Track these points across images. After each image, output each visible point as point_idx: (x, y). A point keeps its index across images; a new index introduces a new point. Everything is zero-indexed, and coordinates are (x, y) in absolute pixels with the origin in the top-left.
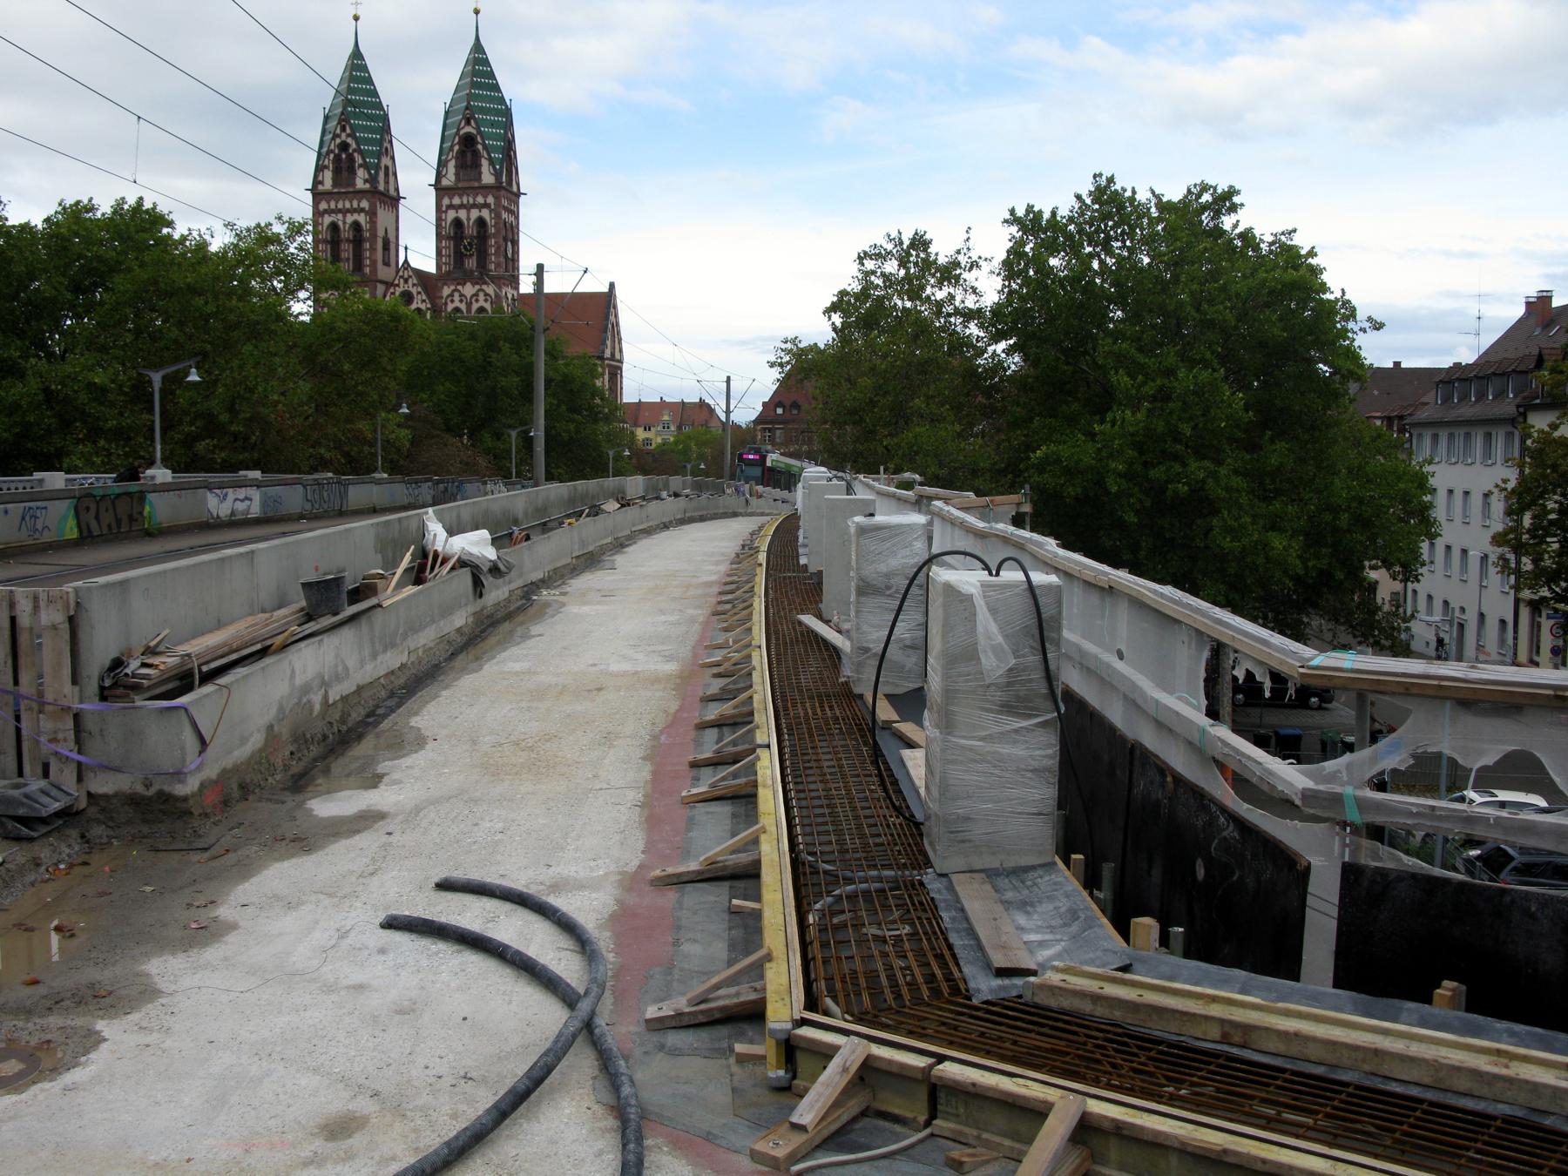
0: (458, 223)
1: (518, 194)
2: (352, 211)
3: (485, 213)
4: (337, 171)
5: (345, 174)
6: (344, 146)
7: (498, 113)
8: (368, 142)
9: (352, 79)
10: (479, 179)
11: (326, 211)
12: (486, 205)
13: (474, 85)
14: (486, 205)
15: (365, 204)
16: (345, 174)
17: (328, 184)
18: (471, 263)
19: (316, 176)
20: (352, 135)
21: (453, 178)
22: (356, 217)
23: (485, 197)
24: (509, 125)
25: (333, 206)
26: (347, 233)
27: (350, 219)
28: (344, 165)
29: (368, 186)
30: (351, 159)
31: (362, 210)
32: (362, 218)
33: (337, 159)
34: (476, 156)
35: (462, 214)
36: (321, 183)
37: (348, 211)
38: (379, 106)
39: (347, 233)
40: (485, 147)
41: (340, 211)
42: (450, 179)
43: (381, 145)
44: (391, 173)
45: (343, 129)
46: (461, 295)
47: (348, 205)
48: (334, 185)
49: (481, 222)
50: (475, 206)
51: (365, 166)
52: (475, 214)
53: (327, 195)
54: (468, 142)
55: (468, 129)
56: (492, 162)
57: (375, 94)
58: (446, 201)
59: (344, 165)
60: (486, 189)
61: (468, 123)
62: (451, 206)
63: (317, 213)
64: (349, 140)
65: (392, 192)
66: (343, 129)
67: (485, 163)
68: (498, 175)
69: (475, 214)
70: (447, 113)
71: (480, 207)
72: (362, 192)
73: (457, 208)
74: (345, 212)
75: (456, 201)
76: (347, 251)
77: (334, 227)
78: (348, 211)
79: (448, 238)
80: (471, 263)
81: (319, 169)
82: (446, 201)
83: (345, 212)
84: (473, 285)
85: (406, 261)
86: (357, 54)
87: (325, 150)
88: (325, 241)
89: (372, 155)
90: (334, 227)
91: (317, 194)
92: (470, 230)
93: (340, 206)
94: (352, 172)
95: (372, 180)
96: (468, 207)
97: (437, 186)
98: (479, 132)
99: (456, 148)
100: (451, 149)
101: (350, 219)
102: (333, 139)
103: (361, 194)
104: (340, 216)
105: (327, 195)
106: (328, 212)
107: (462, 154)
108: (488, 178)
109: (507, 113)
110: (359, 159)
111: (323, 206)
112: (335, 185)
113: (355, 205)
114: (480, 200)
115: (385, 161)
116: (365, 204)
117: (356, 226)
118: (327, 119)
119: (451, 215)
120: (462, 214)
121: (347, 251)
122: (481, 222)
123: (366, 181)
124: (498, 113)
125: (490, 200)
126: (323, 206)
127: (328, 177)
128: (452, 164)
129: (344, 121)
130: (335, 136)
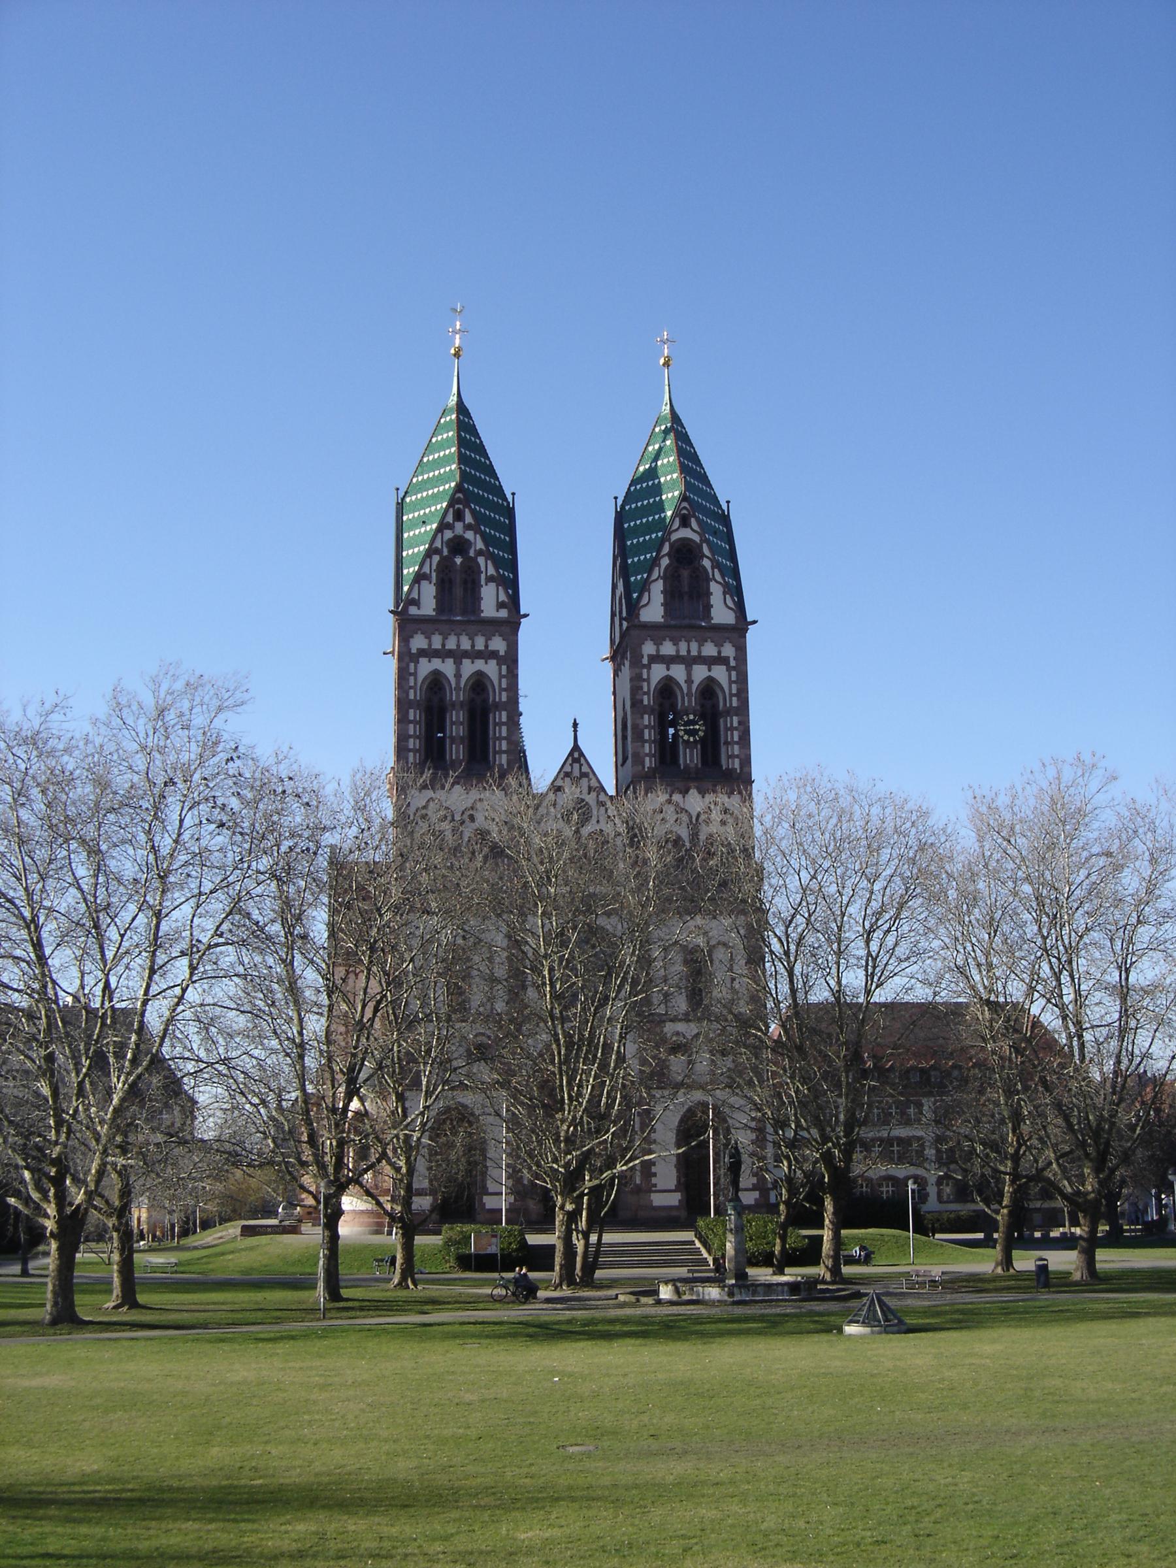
0: (667, 688)
2: (475, 655)
5: (458, 591)
6: (459, 546)
11: (422, 653)
12: (720, 660)
15: (498, 644)
16: (458, 591)
17: (428, 606)
18: (689, 758)
21: (661, 611)
22: (480, 665)
23: (719, 645)
27: (469, 668)
28: (458, 579)
29: (503, 613)
31: (494, 655)
32: (491, 669)
33: (445, 568)
35: (678, 672)
36: (416, 603)
37: (466, 654)
40: (716, 565)
41: (449, 654)
42: (653, 611)
45: (459, 516)
46: (680, 810)
47: (466, 644)
52: (700, 673)
59: (458, 579)
62: (656, 658)
63: (406, 659)
64: (469, 535)
66: (459, 516)
67: (716, 590)
69: (700, 673)
71: (710, 662)
73: (668, 661)
74: (458, 656)
75: (668, 649)
76: (456, 725)
77: (436, 682)
78: (466, 654)
80: (689, 758)
82: (648, 648)
83: (458, 656)
84: (702, 792)
90: (436, 682)
91: (407, 621)
92: (687, 700)
93: (451, 644)
96: (689, 662)
98: (708, 541)
99: (665, 562)
100: (655, 562)
101: (469, 668)
102: (440, 530)
103: (493, 626)
104: (450, 661)
108: (721, 614)
110: (487, 568)
111: (418, 642)
114: (710, 650)
116: (498, 644)
117: (479, 683)
119: (658, 672)
120: (678, 672)
121: (456, 725)
122: (709, 689)
123: (500, 605)
125: (728, 651)
126: (418, 642)
127: (429, 592)
128: (657, 588)
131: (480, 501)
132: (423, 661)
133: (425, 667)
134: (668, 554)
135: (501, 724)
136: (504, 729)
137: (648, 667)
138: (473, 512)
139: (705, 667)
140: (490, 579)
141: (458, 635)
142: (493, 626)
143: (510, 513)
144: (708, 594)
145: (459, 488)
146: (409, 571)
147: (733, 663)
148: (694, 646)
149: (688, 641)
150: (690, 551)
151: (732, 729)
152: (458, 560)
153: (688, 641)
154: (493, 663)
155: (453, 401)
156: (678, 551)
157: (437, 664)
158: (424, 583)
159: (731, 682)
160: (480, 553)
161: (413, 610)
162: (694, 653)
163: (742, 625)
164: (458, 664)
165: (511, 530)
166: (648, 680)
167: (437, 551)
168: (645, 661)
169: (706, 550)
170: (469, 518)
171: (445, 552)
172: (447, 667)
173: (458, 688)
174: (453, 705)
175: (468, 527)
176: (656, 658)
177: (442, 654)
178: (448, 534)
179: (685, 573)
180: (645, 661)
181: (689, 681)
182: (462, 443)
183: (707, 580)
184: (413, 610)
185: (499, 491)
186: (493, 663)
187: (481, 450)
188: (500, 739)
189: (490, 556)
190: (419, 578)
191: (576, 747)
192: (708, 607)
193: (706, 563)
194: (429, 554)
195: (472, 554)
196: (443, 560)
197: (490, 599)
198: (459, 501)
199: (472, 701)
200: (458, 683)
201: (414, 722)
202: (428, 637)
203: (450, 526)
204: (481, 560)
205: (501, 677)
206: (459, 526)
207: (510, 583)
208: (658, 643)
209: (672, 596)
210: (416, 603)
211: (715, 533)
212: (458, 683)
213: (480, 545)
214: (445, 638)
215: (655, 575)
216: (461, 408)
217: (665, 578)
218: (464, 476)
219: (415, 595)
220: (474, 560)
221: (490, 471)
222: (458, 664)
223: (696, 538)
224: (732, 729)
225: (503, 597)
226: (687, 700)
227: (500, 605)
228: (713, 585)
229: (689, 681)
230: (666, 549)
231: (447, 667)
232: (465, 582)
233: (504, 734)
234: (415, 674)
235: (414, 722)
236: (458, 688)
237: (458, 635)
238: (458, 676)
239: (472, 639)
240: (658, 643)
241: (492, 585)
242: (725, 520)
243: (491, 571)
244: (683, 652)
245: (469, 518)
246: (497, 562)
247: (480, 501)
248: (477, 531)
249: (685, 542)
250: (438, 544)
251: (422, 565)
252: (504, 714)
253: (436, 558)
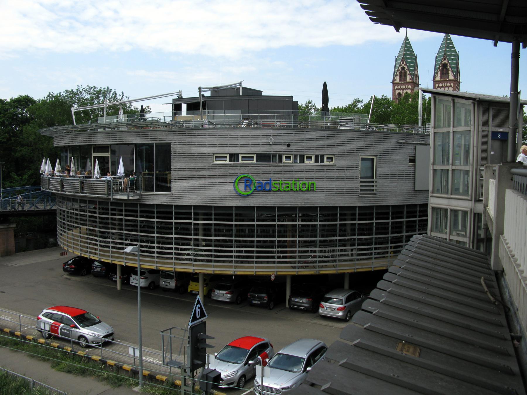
1: (460, 82)
2: (406, 89)
4: (401, 76)
5: (403, 77)
6: (403, 68)
7: (454, 56)
8: (411, 67)
9: (405, 47)
10: (448, 78)
11: (397, 89)
12: (450, 86)
13: (447, 47)
15: (410, 87)
16: (403, 77)
17: (398, 80)
19: (394, 78)
20: (406, 65)
22: (407, 90)
24: (457, 60)
25: (399, 87)
27: (405, 91)
28: (403, 75)
30: (405, 72)
31: (409, 88)
32: (409, 91)
33: (401, 72)
34: (447, 70)
36: (396, 80)
38: (414, 55)
40: (451, 67)
41: (401, 89)
42: (438, 78)
43: (414, 67)
44: (417, 76)
45: (403, 63)
47: (404, 87)
48: (400, 81)
50: (447, 86)
51: (410, 74)
53: (398, 84)
54: (445, 65)
55: (445, 62)
56: (453, 72)
57: (412, 51)
58: (437, 85)
59: (403, 75)
60: (450, 81)
61: (445, 59)
63: (394, 90)
65: (417, 83)
66: (403, 63)
67: (450, 72)
68: (454, 76)
70: (436, 56)
72: (409, 83)
75: (441, 85)
77: (399, 94)
78: (404, 89)
81: (395, 76)
82: (437, 85)
83: (403, 89)
86: (407, 39)
87: (396, 70)
88: (397, 99)
89: (412, 70)
90: (399, 94)
91: (394, 84)
93: (402, 87)
94: (405, 76)
95: (412, 79)
97: (434, 80)
98: (449, 62)
100: (439, 67)
101: (405, 91)
102: (400, 66)
105: (398, 84)
106: (398, 89)
107: (442, 70)
108: (451, 77)
109: (457, 56)
110: (408, 72)
111: (396, 87)
113: (407, 87)
114: (448, 85)
115: (416, 73)
116: (410, 87)
118: (396, 60)
124: (454, 56)
125: (452, 84)
126: (396, 87)
127: (398, 78)
128: (439, 73)
129: (403, 60)
131: (408, 59)
133: (397, 92)
155: (404, 37)
157: (399, 91)
172: (401, 91)
176: (438, 87)
177: (401, 89)
193: (449, 67)
194: (398, 71)
208: (439, 84)
209: (441, 74)
211: (453, 60)
227: (410, 79)
240: (439, 84)
247: (408, 59)
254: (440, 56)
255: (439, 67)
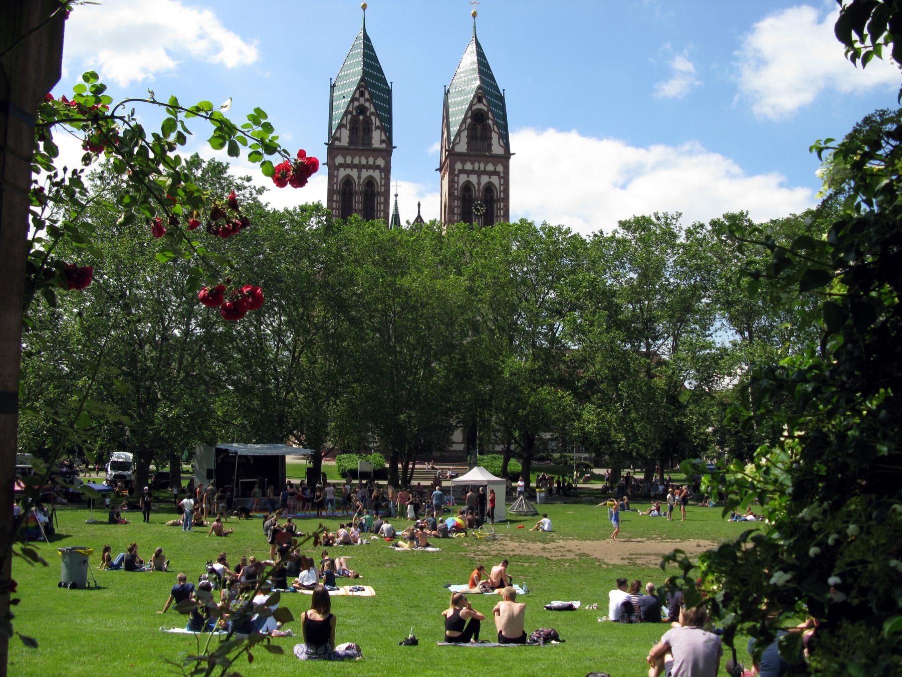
0: (467, 187)
2: (368, 167)
3: (495, 180)
4: (353, 131)
5: (361, 133)
6: (362, 110)
11: (341, 165)
12: (495, 173)
14: (495, 173)
15: (381, 162)
16: (361, 133)
17: (345, 141)
22: (370, 172)
23: (495, 165)
25: (349, 160)
26: (358, 188)
27: (365, 174)
28: (360, 127)
29: (384, 146)
31: (378, 167)
32: (376, 174)
33: (354, 121)
35: (473, 179)
36: (339, 139)
39: (358, 188)
40: (495, 123)
41: (355, 166)
45: (362, 94)
47: (364, 161)
49: (489, 188)
52: (485, 179)
53: (343, 150)
58: (458, 166)
59: (360, 127)
61: (480, 100)
62: (462, 171)
64: (367, 104)
66: (362, 94)
67: (495, 136)
69: (485, 179)
71: (490, 174)
73: (468, 173)
74: (360, 167)
75: (468, 166)
77: (348, 181)
78: (364, 167)
79: (458, 198)
82: (458, 166)
83: (360, 167)
85: (419, 219)
87: (339, 112)
88: (338, 192)
90: (348, 181)
92: (478, 194)
93: (356, 161)
94: (368, 131)
96: (479, 173)
98: (491, 111)
99: (469, 121)
101: (365, 174)
102: (352, 101)
103: (378, 152)
104: (355, 170)
105: (343, 150)
108: (497, 149)
111: (339, 160)
112: (351, 142)
114: (490, 167)
116: (381, 162)
117: (370, 182)
119: (463, 178)
120: (473, 179)
122: (489, 188)
123: (382, 142)
125: (500, 168)
126: (339, 160)
127: (345, 134)
128: (465, 134)
130: (353, 100)
132: (341, 170)
133: (342, 173)
134: (471, 117)
135: (381, 203)
136: (382, 206)
137: (458, 175)
138: (370, 93)
139: (487, 177)
140: (377, 128)
141: (360, 157)
142: (378, 152)
143: (389, 92)
144: (491, 138)
145: (362, 79)
146: (336, 123)
147: (502, 175)
148: (482, 165)
149: (479, 163)
150: (482, 115)
151: (500, 209)
152: (361, 118)
153: (479, 163)
154: (377, 171)
156: (476, 115)
158: (343, 129)
159: (500, 185)
160: (372, 114)
161: (337, 143)
162: (482, 169)
163: (507, 155)
164: (359, 172)
165: (389, 102)
166: (458, 183)
167: (350, 113)
168: (456, 172)
169: (490, 115)
170: (367, 96)
171: (355, 113)
172: (354, 173)
173: (359, 184)
174: (356, 193)
175: (367, 100)
176: (462, 171)
177: (352, 166)
178: (356, 104)
179: (479, 127)
180: (456, 172)
181: (479, 183)
182: (365, 55)
183: (490, 131)
184: (337, 143)
185: (384, 81)
186: (377, 171)
187: (375, 59)
188: (381, 211)
189: (378, 116)
190: (341, 126)
191: (419, 217)
192: (490, 145)
193: (490, 122)
194: (346, 113)
195: (368, 114)
196: (353, 116)
197: (377, 138)
198: (362, 86)
199: (344, 190)
200: (359, 181)
201: (336, 201)
202: (345, 158)
203: (357, 100)
204: (373, 118)
205: (381, 179)
206: (362, 100)
207: (388, 130)
208: (463, 163)
210: (339, 139)
211: (496, 106)
212: (359, 181)
213: (373, 110)
214: (353, 158)
215: (463, 128)
216: (366, 38)
217: (468, 129)
218: (365, 73)
219: (338, 135)
220: (370, 118)
221: (380, 70)
222: (359, 172)
223: (485, 109)
224: (500, 209)
225: (384, 137)
226: (478, 194)
227: (382, 142)
228: (493, 133)
229: (479, 183)
230: (470, 114)
231: (354, 173)
232: (364, 129)
233: (382, 208)
234: (337, 177)
235: (336, 201)
236: (359, 184)
237: (360, 157)
238: (359, 178)
239: (367, 159)
240: (463, 163)
241: (378, 131)
242: (502, 99)
243: (378, 123)
244: (476, 168)
245: (367, 96)
246: (381, 119)
248: (371, 102)
249: (480, 110)
250: (351, 109)
251: (342, 120)
252: (382, 198)
253: (350, 116)
254: (460, 93)
255: (464, 121)
